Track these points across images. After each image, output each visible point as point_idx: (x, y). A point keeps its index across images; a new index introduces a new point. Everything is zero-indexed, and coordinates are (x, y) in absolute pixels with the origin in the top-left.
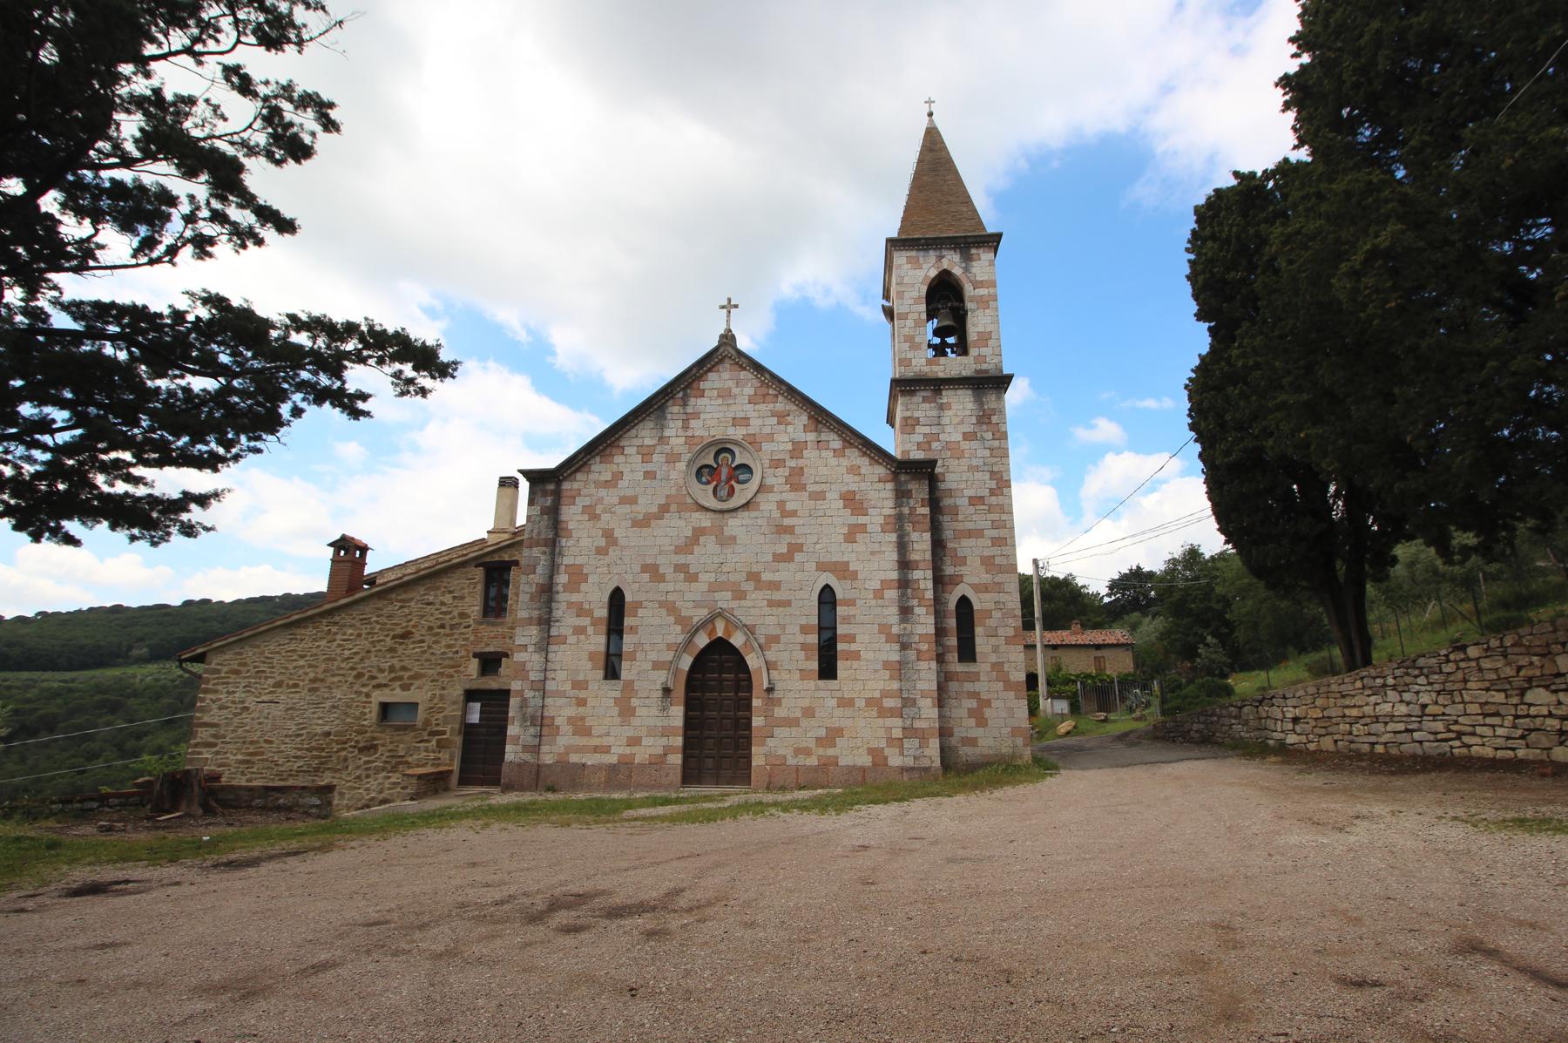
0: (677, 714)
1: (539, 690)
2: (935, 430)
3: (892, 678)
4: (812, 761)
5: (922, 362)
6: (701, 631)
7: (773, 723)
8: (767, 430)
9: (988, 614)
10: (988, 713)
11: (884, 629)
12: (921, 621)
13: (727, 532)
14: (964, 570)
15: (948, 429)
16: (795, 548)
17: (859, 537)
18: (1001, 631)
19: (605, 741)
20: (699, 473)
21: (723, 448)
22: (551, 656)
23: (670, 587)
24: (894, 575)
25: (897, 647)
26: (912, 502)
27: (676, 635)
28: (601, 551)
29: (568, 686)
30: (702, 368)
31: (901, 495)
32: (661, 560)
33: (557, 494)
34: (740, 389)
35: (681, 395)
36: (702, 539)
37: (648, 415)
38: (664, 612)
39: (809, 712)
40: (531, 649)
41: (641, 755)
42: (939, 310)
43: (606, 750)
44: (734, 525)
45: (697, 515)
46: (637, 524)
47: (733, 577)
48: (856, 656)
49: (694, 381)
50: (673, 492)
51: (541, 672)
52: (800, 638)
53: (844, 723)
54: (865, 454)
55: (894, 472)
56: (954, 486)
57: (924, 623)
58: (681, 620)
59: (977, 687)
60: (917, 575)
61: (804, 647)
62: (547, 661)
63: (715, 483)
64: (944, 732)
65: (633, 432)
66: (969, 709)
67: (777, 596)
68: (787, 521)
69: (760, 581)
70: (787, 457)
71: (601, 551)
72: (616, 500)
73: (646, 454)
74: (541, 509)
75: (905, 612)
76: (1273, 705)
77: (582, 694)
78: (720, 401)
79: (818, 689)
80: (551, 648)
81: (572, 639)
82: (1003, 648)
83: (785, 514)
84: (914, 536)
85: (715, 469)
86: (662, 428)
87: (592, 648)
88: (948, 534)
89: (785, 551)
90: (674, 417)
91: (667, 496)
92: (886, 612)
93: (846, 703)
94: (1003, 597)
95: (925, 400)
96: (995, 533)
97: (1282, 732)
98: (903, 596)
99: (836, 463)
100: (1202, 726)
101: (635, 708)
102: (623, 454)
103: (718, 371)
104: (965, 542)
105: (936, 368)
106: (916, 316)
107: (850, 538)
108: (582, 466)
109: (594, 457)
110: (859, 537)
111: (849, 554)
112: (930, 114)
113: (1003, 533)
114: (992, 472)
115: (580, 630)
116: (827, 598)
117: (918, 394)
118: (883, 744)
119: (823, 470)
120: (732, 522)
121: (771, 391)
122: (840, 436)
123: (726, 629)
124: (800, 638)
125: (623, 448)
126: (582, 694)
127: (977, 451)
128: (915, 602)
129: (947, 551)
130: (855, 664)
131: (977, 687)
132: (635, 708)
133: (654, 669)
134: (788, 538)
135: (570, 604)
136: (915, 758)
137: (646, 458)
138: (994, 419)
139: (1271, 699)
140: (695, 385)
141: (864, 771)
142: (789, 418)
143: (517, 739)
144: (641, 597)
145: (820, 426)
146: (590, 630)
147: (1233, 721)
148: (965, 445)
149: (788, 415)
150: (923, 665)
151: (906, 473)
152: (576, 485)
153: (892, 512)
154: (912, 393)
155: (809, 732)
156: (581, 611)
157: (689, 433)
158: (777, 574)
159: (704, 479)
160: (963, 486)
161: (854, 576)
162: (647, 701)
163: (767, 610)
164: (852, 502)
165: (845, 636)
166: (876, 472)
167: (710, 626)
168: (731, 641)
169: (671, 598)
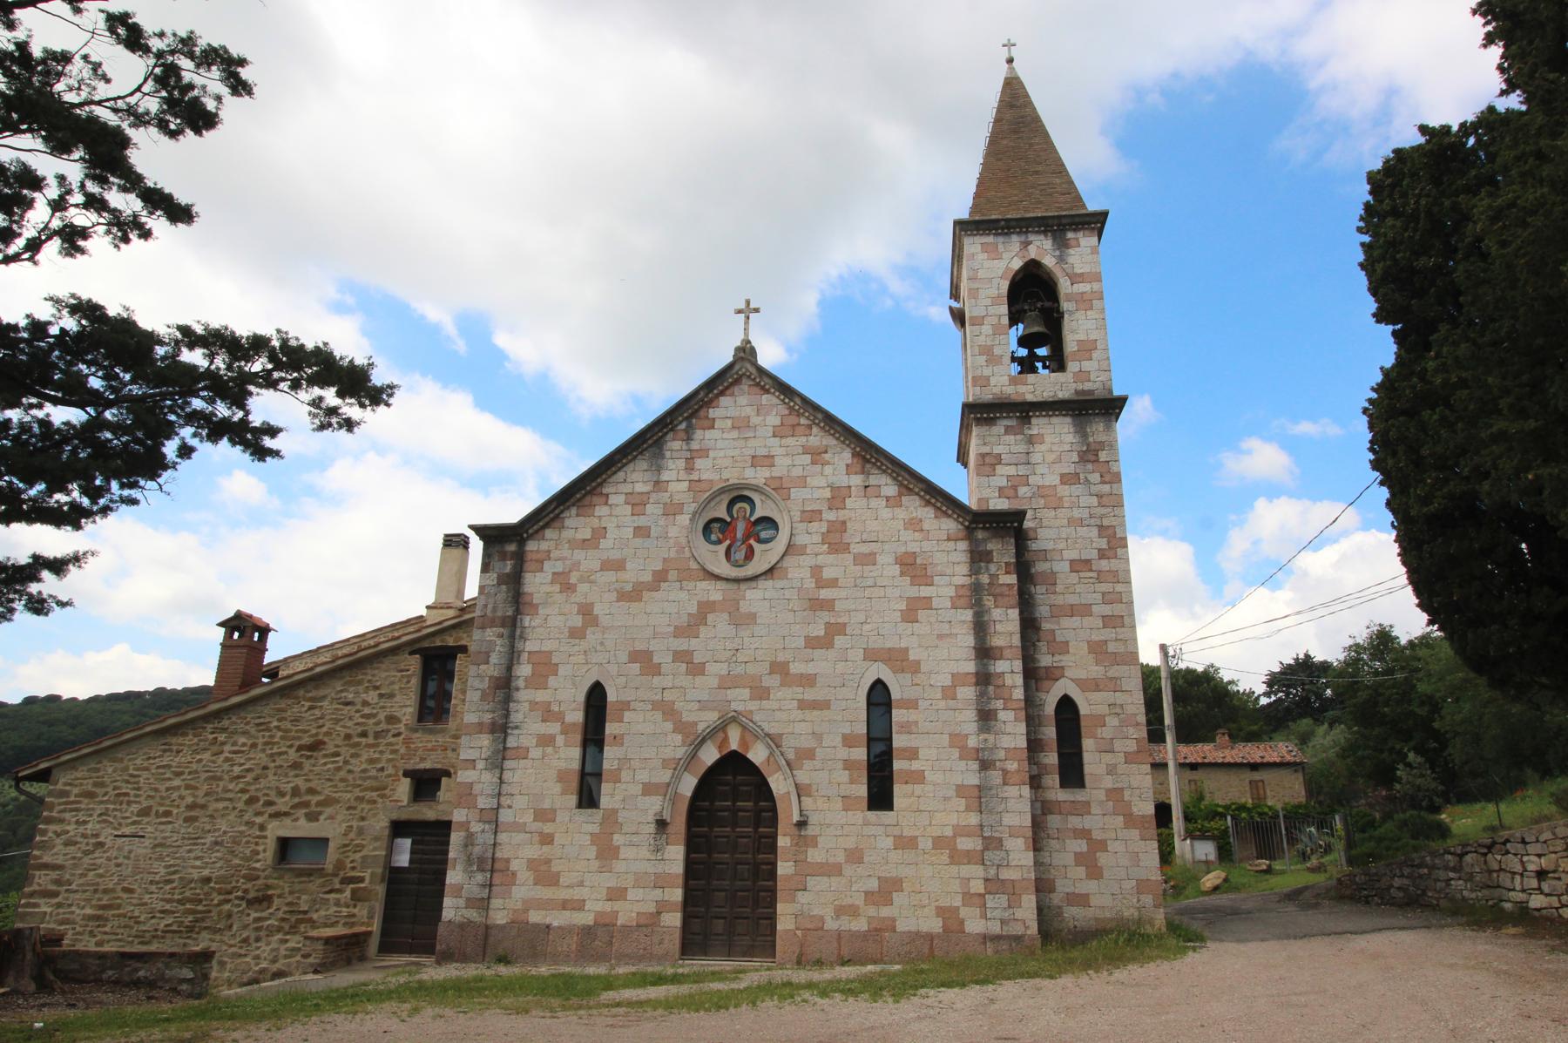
0: (676, 855)
1: (489, 822)
2: (1022, 470)
3: (968, 809)
4: (860, 925)
5: (1003, 381)
6: (709, 742)
7: (806, 870)
8: (797, 472)
9: (1100, 721)
10: (1103, 859)
11: (957, 740)
12: (1008, 731)
13: (744, 607)
14: (1065, 660)
15: (1040, 469)
17: (922, 614)
18: (1118, 745)
19: (576, 894)
20: (707, 529)
21: (739, 497)
22: (507, 775)
23: (667, 681)
24: (971, 667)
25: (975, 765)
26: (993, 568)
27: (676, 747)
28: (576, 634)
29: (528, 818)
30: (711, 391)
31: (978, 558)
32: (654, 645)
33: (520, 558)
34: (761, 418)
35: (683, 426)
36: (710, 618)
37: (641, 453)
38: (658, 716)
39: (855, 856)
40: (481, 765)
41: (627, 913)
42: (1025, 311)
43: (579, 906)
44: (754, 598)
46: (623, 596)
47: (752, 669)
48: (918, 778)
49: (701, 407)
50: (673, 554)
51: (492, 796)
52: (843, 753)
53: (903, 872)
54: (928, 503)
55: (967, 528)
56: (1050, 546)
57: (1012, 733)
58: (681, 727)
59: (1086, 822)
60: (1001, 666)
61: (848, 765)
62: (502, 782)
63: (728, 542)
64: (1043, 886)
65: (621, 475)
66: (1076, 853)
67: (810, 694)
68: (825, 594)
69: (787, 674)
70: (824, 507)
71: (576, 634)
72: (597, 565)
73: (638, 504)
74: (498, 578)
75: (986, 717)
76: (1508, 852)
77: (548, 828)
78: (735, 434)
79: (866, 823)
80: (508, 764)
81: (535, 753)
82: (1122, 768)
83: (821, 583)
84: (997, 613)
85: (729, 524)
86: (659, 470)
87: (563, 765)
88: (1042, 611)
89: (822, 633)
90: (675, 455)
92: (960, 717)
93: (905, 843)
94: (1120, 698)
95: (1008, 430)
96: (1107, 610)
97: (1523, 891)
98: (982, 695)
99: (890, 516)
100: (1406, 881)
101: (618, 847)
102: (606, 504)
103: (732, 395)
104: (1066, 622)
105: (1022, 389)
106: (995, 320)
107: (910, 616)
108: (553, 520)
109: (568, 508)
110: (922, 614)
111: (909, 639)
112: (1010, 61)
113: (1118, 609)
114: (1101, 527)
115: (546, 741)
116: (879, 697)
117: (998, 422)
118: (957, 902)
119: (873, 525)
120: (750, 594)
121: (803, 421)
122: (895, 479)
123: (743, 742)
124: (843, 753)
125: (607, 495)
126: (548, 828)
127: (1081, 499)
128: (999, 704)
129: (1041, 633)
130: (918, 789)
131: (1086, 822)
132: (618, 847)
133: (644, 794)
134: (825, 617)
135: (534, 705)
136: (1003, 922)
137: (637, 509)
138: (1103, 456)
139: (1504, 844)
140: (702, 413)
141: (932, 940)
142: (827, 456)
143: (458, 890)
145: (868, 466)
146: (560, 740)
147: (1451, 875)
148: (1064, 491)
149: (826, 452)
150: (1012, 791)
151: (984, 528)
152: (544, 546)
153: (966, 581)
154: (990, 422)
155: (859, 883)
156: (548, 714)
157: (695, 476)
159: (713, 537)
160: (1062, 545)
161: (915, 668)
162: (635, 839)
163: (798, 715)
164: (912, 567)
165: (904, 750)
166: (944, 526)
167: (721, 735)
168: (750, 756)
169: (668, 696)
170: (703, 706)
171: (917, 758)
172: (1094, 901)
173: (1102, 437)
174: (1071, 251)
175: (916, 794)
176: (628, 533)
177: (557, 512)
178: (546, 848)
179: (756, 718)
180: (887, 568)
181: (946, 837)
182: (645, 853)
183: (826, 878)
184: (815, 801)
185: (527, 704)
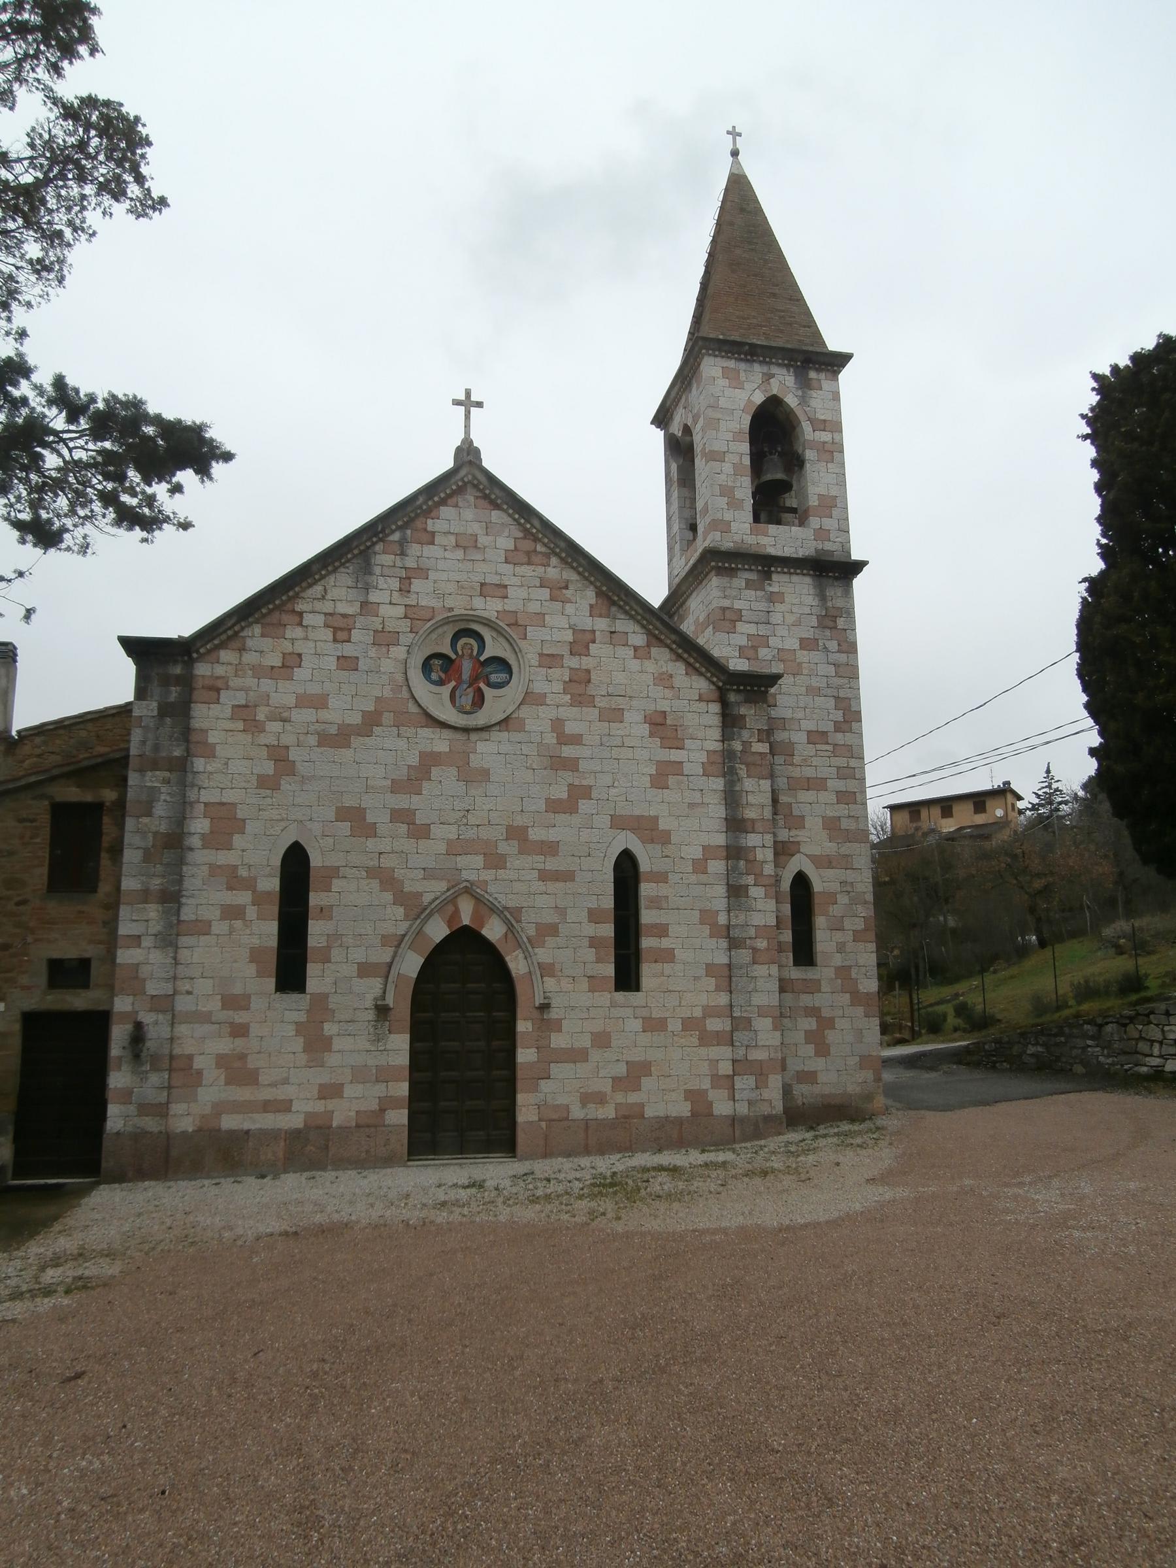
2: (763, 630)
3: (718, 989)
4: (607, 1112)
6: (436, 915)
7: (550, 1057)
8: (534, 607)
9: (832, 898)
10: (831, 1036)
11: (707, 917)
12: (759, 907)
13: (475, 761)
15: (781, 631)
16: (579, 793)
17: (672, 780)
18: (847, 924)
19: (281, 1093)
20: (426, 667)
22: (184, 954)
23: (384, 845)
24: (720, 840)
25: (724, 944)
26: (745, 734)
29: (215, 1005)
32: (367, 802)
36: (435, 772)
37: (342, 565)
38: (375, 884)
39: (602, 1040)
41: (343, 1113)
43: (285, 1106)
44: (486, 751)
45: (426, 732)
46: (325, 740)
47: (484, 833)
48: (668, 956)
50: (387, 693)
52: (590, 930)
54: (679, 657)
58: (402, 898)
59: (817, 1000)
61: (594, 942)
63: (453, 683)
65: (317, 589)
66: (806, 1031)
67: (552, 864)
68: (568, 751)
69: (526, 840)
70: (565, 651)
71: (267, 783)
72: (291, 700)
75: (736, 892)
76: (1150, 1023)
77: (240, 1017)
79: (613, 1005)
81: (220, 927)
82: (850, 946)
83: (565, 739)
84: (748, 784)
86: (367, 589)
89: (565, 796)
91: (378, 699)
93: (654, 1025)
94: (850, 876)
96: (840, 785)
97: (1161, 1056)
99: (638, 668)
101: (330, 1038)
105: (764, 540)
107: (659, 781)
110: (672, 780)
115: (233, 913)
117: (740, 574)
118: (706, 1084)
119: (620, 677)
120: (481, 747)
123: (476, 915)
124: (590, 930)
128: (750, 880)
131: (817, 1000)
132: (330, 1038)
134: (568, 777)
137: (341, 635)
138: (841, 623)
139: (1148, 1015)
141: (681, 1124)
142: (568, 593)
144: (334, 860)
147: (1089, 1042)
148: (803, 656)
150: (760, 970)
153: (718, 746)
154: (731, 572)
157: (412, 601)
158: (551, 831)
159: (434, 676)
161: (664, 838)
163: (539, 886)
164: (659, 724)
165: (655, 926)
168: (484, 932)
169: (386, 862)
170: (429, 874)
171: (667, 936)
172: (822, 1078)
173: (839, 603)
174: (814, 393)
175: (667, 972)
176: (332, 663)
177: (236, 628)
178: (239, 1042)
179: (491, 889)
180: (635, 727)
181: (696, 1018)
182: (363, 1043)
183: (572, 1065)
184: (559, 982)
185: (205, 868)
